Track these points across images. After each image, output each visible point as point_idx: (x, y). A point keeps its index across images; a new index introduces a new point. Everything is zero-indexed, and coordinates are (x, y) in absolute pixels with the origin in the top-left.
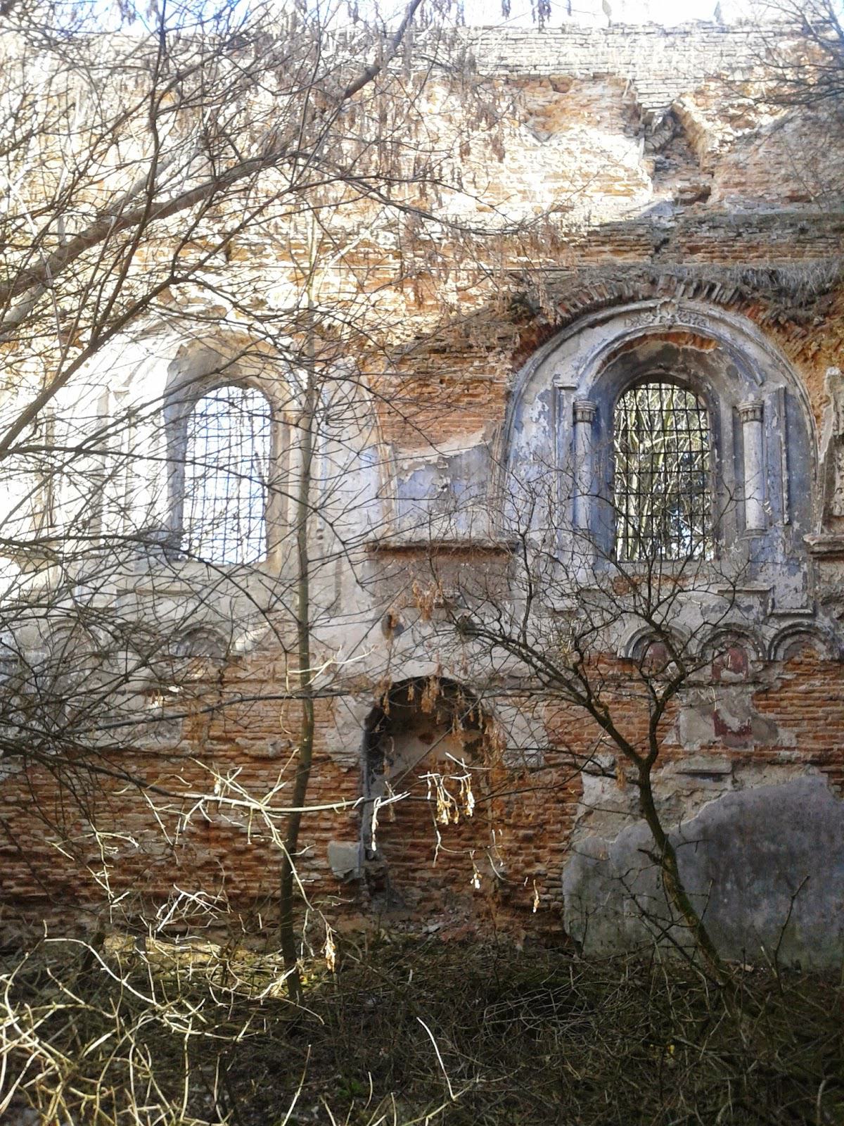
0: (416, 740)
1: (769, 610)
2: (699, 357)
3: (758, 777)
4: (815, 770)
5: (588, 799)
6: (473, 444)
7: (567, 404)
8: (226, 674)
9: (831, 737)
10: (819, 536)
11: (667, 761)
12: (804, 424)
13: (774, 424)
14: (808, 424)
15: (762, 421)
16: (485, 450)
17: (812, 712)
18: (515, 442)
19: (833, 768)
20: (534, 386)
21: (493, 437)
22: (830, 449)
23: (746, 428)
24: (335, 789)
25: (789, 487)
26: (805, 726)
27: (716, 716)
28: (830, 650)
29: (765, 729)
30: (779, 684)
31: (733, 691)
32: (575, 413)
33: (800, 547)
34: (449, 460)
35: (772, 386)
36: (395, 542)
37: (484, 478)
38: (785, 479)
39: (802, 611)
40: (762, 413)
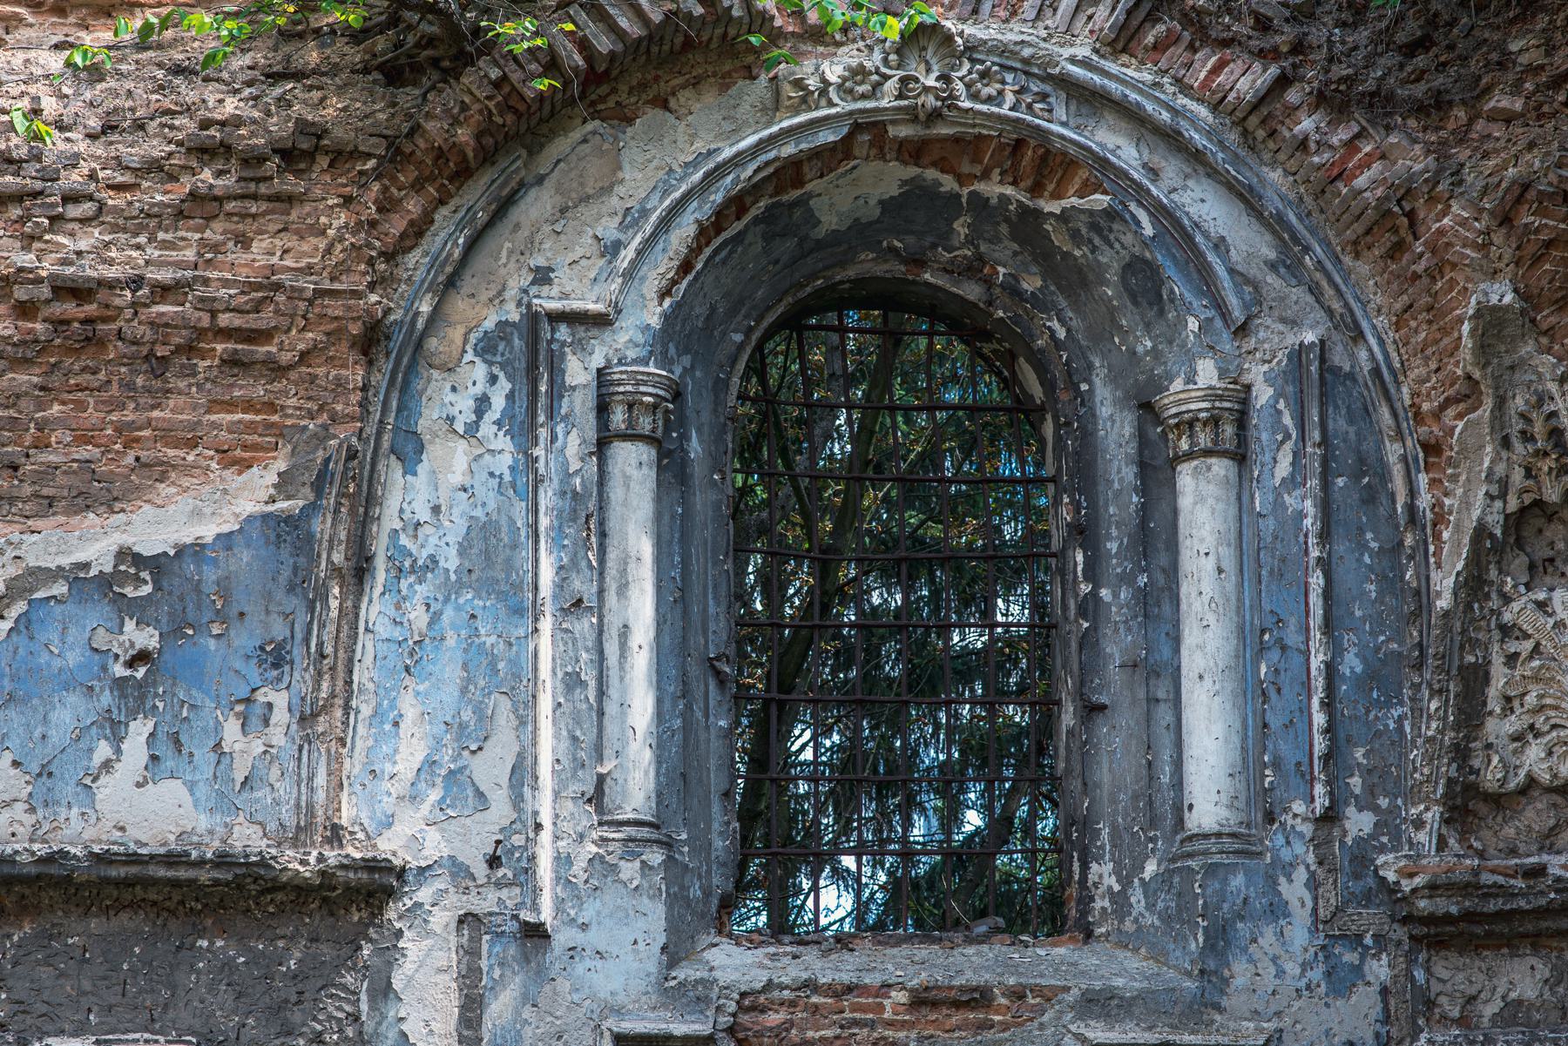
2: (1027, 226)
6: (248, 507)
7: (578, 372)
10: (1432, 860)
12: (1384, 475)
13: (1283, 468)
14: (1397, 472)
15: (1240, 457)
16: (283, 532)
20: (459, 305)
21: (318, 487)
22: (1476, 561)
23: (1186, 478)
25: (1330, 688)
32: (603, 409)
33: (1367, 898)
34: (157, 565)
35: (1277, 340)
37: (279, 630)
38: (1317, 661)
40: (1242, 420)
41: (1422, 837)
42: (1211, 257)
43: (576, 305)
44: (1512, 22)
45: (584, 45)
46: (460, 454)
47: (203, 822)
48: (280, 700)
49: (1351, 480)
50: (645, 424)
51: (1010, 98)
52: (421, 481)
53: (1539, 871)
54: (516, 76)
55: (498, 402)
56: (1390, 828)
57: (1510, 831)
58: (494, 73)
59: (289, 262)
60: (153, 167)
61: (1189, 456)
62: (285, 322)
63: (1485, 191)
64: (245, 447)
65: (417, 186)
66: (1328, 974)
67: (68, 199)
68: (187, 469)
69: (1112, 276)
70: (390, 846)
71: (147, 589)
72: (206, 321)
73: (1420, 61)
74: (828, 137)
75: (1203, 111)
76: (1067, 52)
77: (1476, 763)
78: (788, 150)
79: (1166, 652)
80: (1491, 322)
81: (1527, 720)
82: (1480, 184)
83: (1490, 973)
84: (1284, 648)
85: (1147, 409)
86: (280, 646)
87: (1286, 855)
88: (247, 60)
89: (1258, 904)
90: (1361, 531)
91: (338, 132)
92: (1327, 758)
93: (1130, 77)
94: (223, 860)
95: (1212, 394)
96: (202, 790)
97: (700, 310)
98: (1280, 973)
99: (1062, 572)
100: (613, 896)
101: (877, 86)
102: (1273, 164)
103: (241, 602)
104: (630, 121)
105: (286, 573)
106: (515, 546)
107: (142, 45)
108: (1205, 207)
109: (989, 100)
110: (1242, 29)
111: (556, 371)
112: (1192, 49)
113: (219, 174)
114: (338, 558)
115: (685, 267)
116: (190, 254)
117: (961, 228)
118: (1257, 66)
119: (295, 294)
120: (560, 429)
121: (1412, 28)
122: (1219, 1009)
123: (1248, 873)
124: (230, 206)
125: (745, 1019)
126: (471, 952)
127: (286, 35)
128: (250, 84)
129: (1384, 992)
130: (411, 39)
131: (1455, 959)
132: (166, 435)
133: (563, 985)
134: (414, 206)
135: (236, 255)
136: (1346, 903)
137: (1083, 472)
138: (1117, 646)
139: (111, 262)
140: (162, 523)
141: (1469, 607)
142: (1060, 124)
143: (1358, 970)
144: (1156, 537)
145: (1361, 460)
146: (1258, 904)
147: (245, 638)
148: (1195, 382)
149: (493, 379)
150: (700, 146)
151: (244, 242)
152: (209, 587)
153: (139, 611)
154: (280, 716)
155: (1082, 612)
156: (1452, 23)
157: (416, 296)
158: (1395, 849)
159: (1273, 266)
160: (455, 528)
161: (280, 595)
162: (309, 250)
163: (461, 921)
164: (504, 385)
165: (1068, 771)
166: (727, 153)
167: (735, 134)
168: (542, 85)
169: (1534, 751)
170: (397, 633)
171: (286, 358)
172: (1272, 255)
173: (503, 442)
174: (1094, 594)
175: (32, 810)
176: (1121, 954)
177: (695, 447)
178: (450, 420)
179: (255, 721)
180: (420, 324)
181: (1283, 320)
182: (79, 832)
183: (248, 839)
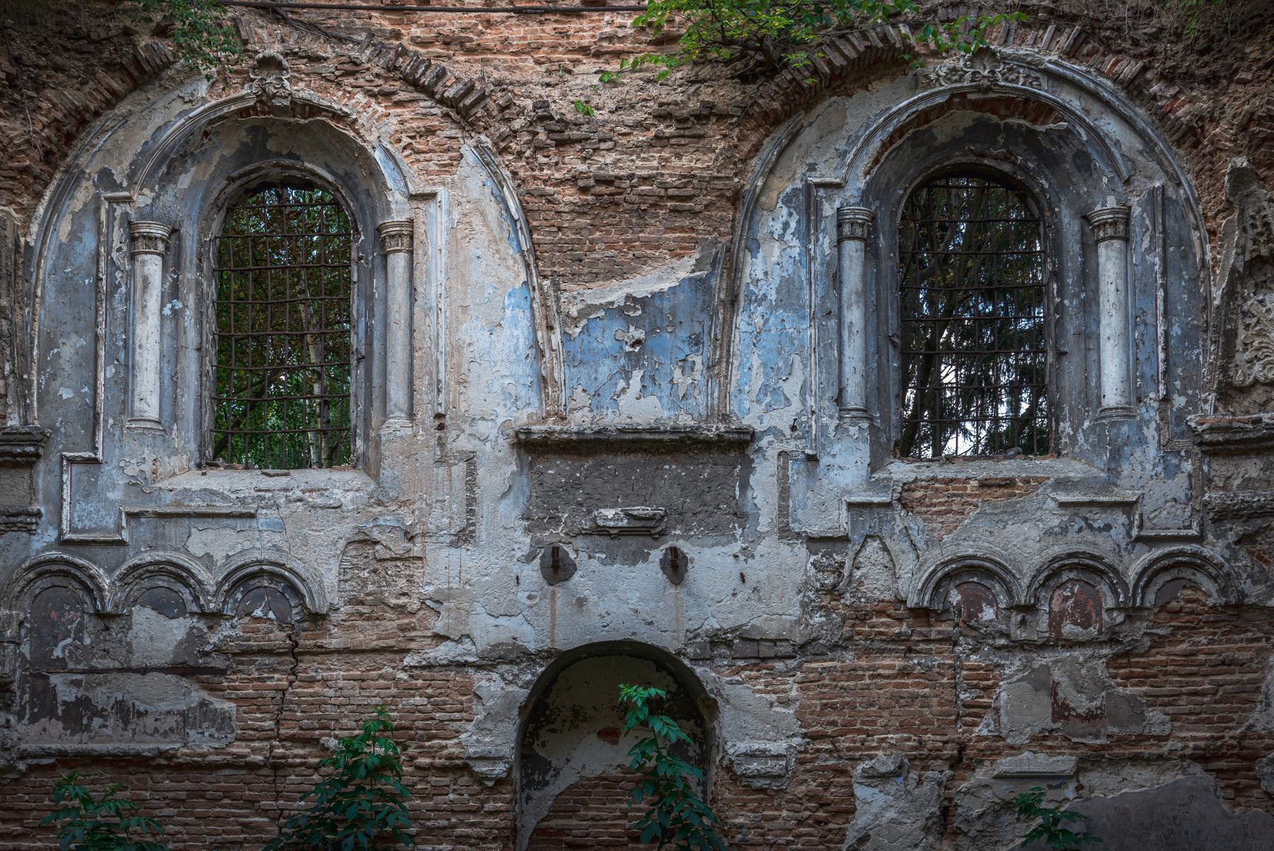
0: (594, 737)
1: (1135, 532)
3: (1112, 781)
4: (1197, 769)
5: (861, 820)
6: (683, 274)
7: (828, 210)
8: (301, 642)
9: (1221, 720)
10: (1211, 418)
11: (980, 762)
12: (1191, 246)
13: (1146, 244)
15: (1127, 239)
16: (699, 285)
17: (1193, 684)
18: (747, 270)
19: (1223, 764)
20: (776, 182)
21: (713, 265)
22: (1231, 284)
23: (1102, 249)
24: (474, 812)
26: (1184, 704)
27: (1053, 691)
28: (1223, 591)
30: (1147, 642)
31: (1078, 654)
32: (840, 226)
33: (1182, 435)
34: (643, 302)
37: (698, 329)
38: (1161, 330)
39: (1183, 532)
40: (1127, 222)
41: (1207, 407)
42: (1113, 149)
43: (827, 180)
44: (1249, 38)
45: (829, 63)
46: (777, 248)
47: (666, 414)
48: (698, 360)
49: (1173, 246)
50: (859, 232)
51: (1022, 80)
52: (759, 260)
53: (1259, 421)
54: (799, 78)
55: (793, 225)
56: (1193, 403)
57: (1246, 403)
58: (789, 77)
59: (699, 165)
60: (639, 125)
61: (1104, 239)
62: (697, 192)
63: (1234, 116)
64: (681, 248)
65: (755, 129)
66: (1165, 469)
67: (601, 140)
68: (655, 259)
69: (1069, 159)
71: (639, 312)
72: (662, 192)
73: (1206, 58)
74: (940, 100)
75: (1109, 83)
76: (1047, 59)
77: (1231, 373)
78: (922, 107)
79: (1094, 328)
80: (1237, 174)
81: (1255, 353)
82: (1233, 112)
83: (1237, 466)
84: (1146, 324)
85: (1086, 219)
86: (698, 336)
87: (1146, 416)
88: (679, 75)
89: (1134, 438)
90: (1181, 271)
91: (720, 106)
92: (1165, 373)
93: (1075, 69)
94: (675, 430)
95: (1113, 211)
96: (665, 400)
97: (883, 180)
98: (1143, 469)
99: (1047, 293)
100: (846, 442)
101: (961, 76)
102: (1141, 106)
103: (681, 316)
104: (851, 96)
105: (700, 303)
106: (801, 288)
107: (633, 71)
108: (1111, 127)
109: (1012, 81)
110: (1127, 45)
111: (818, 209)
112: (1104, 55)
113: (668, 127)
114: (722, 296)
115: (876, 161)
116: (655, 163)
117: (1000, 140)
118: (1133, 62)
119: (701, 179)
120: (821, 236)
121: (1202, 43)
122: (1116, 485)
123: (1130, 425)
124: (672, 141)
125: (905, 494)
126: (784, 468)
127: (696, 63)
128: (680, 86)
129: (1190, 476)
130: (752, 63)
131: (1221, 461)
132: (646, 244)
133: (825, 481)
134: (754, 138)
135: (675, 162)
136: (1173, 437)
137: (1056, 248)
138: (1071, 326)
139: (621, 168)
140: (644, 284)
141: (1228, 304)
142: (1045, 90)
143: (1178, 466)
144: (1089, 276)
145: (1181, 239)
146: (1134, 438)
147: (683, 334)
149: (790, 214)
150: (882, 106)
151: (679, 156)
152: (666, 311)
153: (636, 322)
154: (699, 367)
155: (1056, 311)
156: (1220, 41)
157: (756, 179)
158: (1195, 412)
159: (1141, 153)
160: (775, 282)
161: (697, 313)
162: (708, 160)
163: (780, 454)
164: (796, 216)
165: (1050, 382)
166: (894, 109)
167: (899, 100)
168: (809, 81)
169: (1257, 367)
170: (750, 329)
171: (698, 208)
172: (1141, 147)
173: (795, 242)
174: (1062, 302)
175: (591, 411)
176: (1073, 462)
177: (882, 242)
178: (772, 233)
179: (687, 369)
180: (758, 190)
181: (1146, 177)
182: (612, 419)
183: (686, 421)
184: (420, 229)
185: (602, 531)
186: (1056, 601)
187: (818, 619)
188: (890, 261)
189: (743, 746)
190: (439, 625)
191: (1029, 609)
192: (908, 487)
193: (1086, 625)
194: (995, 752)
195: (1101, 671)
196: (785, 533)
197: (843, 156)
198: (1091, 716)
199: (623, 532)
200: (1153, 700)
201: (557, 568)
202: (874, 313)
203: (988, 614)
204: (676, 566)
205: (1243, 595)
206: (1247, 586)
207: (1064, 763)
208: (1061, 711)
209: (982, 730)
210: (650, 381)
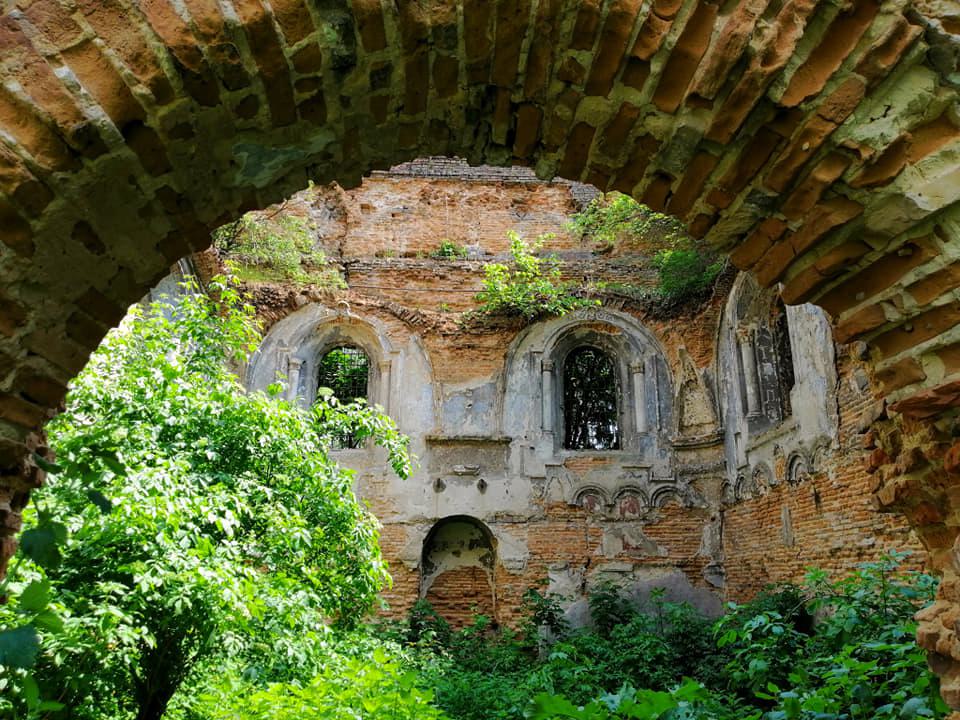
0: (451, 555)
2: (609, 337)
4: (679, 570)
7: (538, 361)
16: (493, 385)
19: (689, 569)
28: (685, 501)
29: (649, 546)
31: (632, 524)
35: (648, 354)
36: (442, 437)
49: (661, 378)
56: (670, 432)
70: (510, 435)
138: (625, 403)
142: (613, 322)
144: (631, 386)
148: (635, 362)
183: (487, 434)
184: (393, 364)
185: (456, 473)
186: (623, 503)
187: (535, 508)
188: (560, 380)
189: (507, 557)
190: (394, 509)
191: (612, 507)
192: (567, 460)
193: (634, 512)
194: (601, 562)
195: (641, 531)
196: (522, 475)
197: (542, 340)
198: (637, 548)
199: (463, 474)
200: (661, 543)
201: (439, 486)
202: (555, 396)
203: (597, 508)
204: (482, 486)
205: (692, 503)
206: (693, 500)
207: (628, 567)
208: (626, 546)
209: (597, 552)
210: (475, 418)
